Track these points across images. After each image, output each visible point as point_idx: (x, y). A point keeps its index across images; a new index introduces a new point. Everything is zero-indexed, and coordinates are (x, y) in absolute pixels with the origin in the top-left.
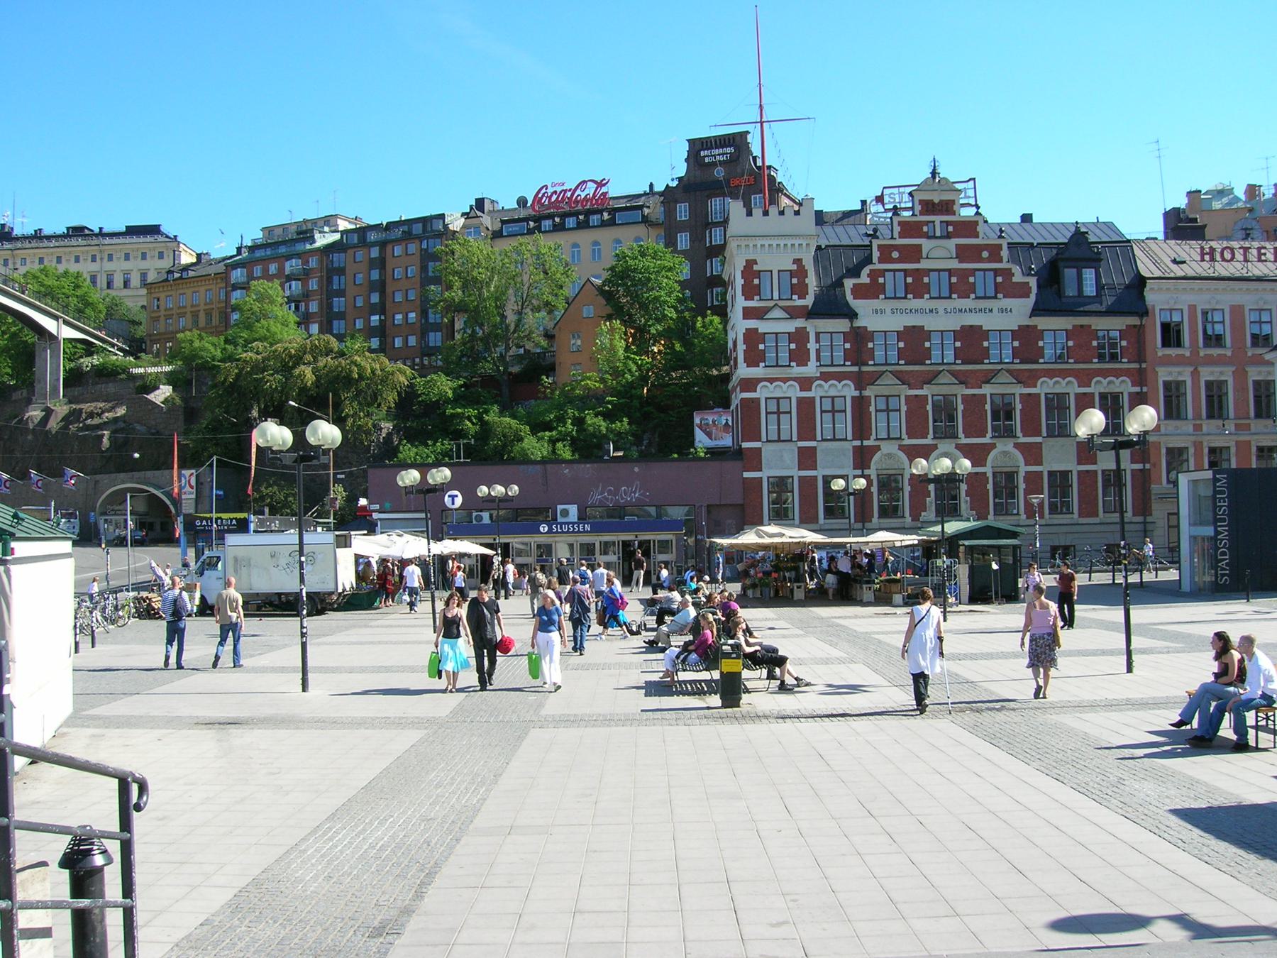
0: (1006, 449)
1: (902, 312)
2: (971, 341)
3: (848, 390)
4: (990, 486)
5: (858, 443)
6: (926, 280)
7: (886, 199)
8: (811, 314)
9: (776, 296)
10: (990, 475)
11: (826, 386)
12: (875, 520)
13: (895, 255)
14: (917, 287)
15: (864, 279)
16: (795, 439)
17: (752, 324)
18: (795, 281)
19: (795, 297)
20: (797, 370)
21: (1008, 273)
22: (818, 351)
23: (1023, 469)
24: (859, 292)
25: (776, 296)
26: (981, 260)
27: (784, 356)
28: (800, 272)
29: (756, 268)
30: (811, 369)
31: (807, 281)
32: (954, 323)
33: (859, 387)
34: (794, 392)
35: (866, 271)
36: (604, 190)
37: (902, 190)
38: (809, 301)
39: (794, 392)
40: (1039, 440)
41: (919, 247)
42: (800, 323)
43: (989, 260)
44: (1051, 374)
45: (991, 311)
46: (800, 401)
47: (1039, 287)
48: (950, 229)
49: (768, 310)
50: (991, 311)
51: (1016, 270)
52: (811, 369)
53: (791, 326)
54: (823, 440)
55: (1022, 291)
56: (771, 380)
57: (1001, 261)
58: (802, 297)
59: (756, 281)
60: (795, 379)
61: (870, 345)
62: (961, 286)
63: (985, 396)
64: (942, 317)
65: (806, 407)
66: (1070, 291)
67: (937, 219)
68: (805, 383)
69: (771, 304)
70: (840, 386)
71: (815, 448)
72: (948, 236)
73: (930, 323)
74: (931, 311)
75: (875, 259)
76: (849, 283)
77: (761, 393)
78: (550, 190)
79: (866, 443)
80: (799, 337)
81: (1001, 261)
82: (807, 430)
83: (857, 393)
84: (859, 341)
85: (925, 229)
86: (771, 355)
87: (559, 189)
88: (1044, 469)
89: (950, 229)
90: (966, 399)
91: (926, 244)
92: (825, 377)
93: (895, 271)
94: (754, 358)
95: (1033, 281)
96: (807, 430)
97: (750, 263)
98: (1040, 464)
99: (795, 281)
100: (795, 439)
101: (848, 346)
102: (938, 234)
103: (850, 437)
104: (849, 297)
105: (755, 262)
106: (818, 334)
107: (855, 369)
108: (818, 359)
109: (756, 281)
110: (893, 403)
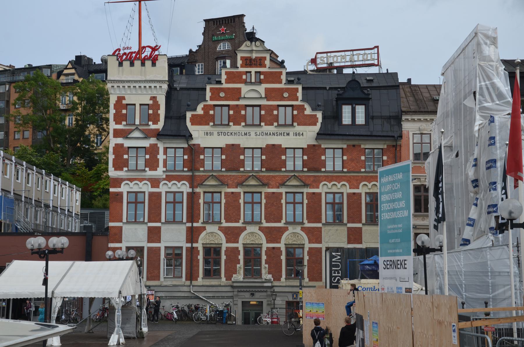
0: (294, 231)
1: (225, 134)
2: (273, 154)
3: (185, 188)
4: (283, 257)
5: (189, 225)
6: (243, 112)
7: (318, 61)
8: (160, 135)
9: (137, 122)
10: (283, 249)
11: (170, 184)
13: (222, 95)
14: (237, 118)
15: (200, 111)
16: (146, 221)
17: (120, 141)
18: (151, 112)
19: (150, 123)
20: (150, 173)
21: (301, 109)
22: (165, 161)
23: (308, 246)
24: (197, 121)
25: (137, 122)
26: (283, 99)
27: (141, 163)
28: (155, 106)
29: (124, 102)
30: (160, 172)
31: (159, 112)
32: (262, 142)
33: (192, 186)
34: (147, 188)
35: (200, 107)
36: (157, 53)
37: (329, 54)
38: (160, 126)
39: (147, 188)
40: (319, 225)
41: (239, 89)
42: (153, 141)
43: (288, 99)
44: (330, 179)
45: (288, 134)
46: (151, 194)
47: (324, 118)
48: (262, 77)
49: (131, 131)
50: (288, 134)
51: (307, 106)
52: (160, 172)
53: (146, 143)
54: (128, 222)
55: (312, 120)
56: (131, 180)
57: (297, 100)
58: (156, 122)
59: (124, 111)
60: (149, 180)
61: (202, 157)
62: (268, 117)
63: (281, 194)
64: (253, 139)
65: (155, 198)
66: (346, 120)
67: (253, 70)
68: (155, 182)
69: (133, 128)
70: (179, 184)
71: (159, 228)
72: (260, 82)
73: (243, 142)
74: (246, 134)
75: (208, 98)
76: (189, 115)
77: (124, 189)
78: (122, 52)
79: (195, 225)
80: (153, 151)
81: (297, 100)
82: (154, 216)
83: (190, 190)
84: (194, 153)
85: (244, 77)
86: (132, 163)
87: (127, 51)
88: (323, 246)
89: (262, 77)
90: (268, 196)
91: (245, 89)
92: (169, 178)
93: (285, 106)
94: (120, 164)
95: (319, 115)
96: (154, 216)
97: (120, 99)
98: (320, 242)
99: (151, 112)
100: (146, 221)
101: (186, 157)
102: (253, 81)
103: (185, 220)
105: (124, 98)
106: (166, 149)
107: (190, 174)
108: (165, 165)
109: (124, 111)
110: (298, 198)
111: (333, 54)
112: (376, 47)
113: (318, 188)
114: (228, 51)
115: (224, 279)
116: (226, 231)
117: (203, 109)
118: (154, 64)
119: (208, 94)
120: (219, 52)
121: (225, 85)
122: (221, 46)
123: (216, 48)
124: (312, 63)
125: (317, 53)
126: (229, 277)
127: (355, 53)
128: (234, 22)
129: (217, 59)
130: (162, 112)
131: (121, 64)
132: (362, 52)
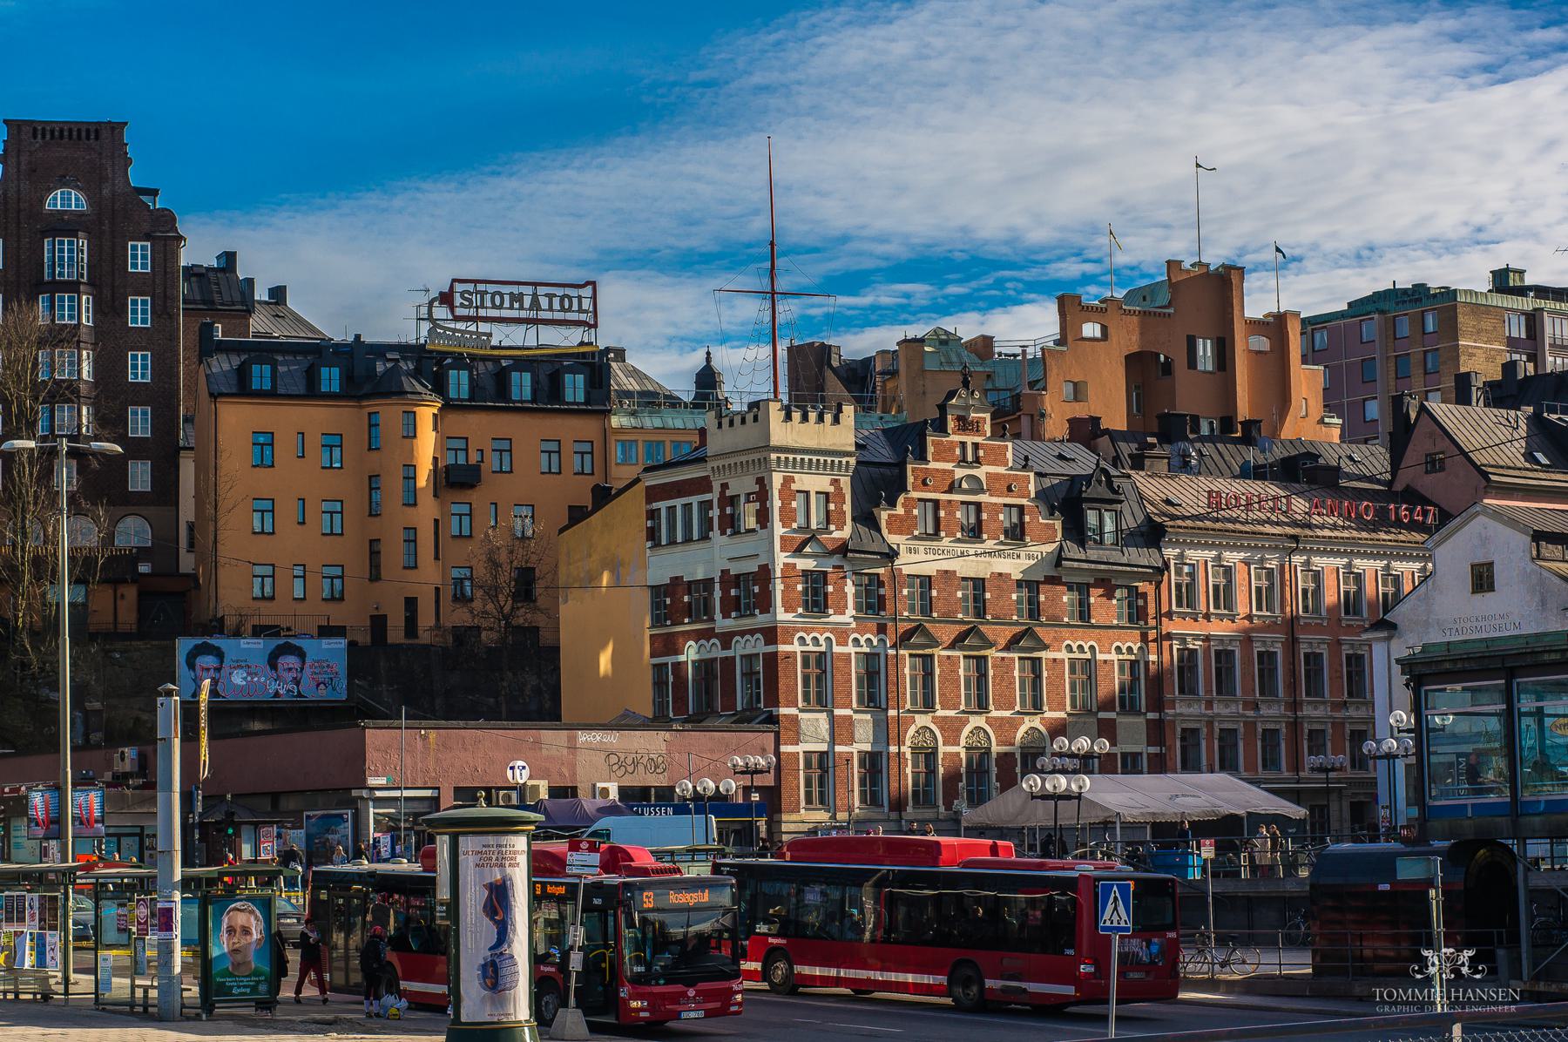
7: (458, 300)
12: (909, 809)
25: (814, 526)
29: (794, 487)
35: (901, 499)
37: (481, 287)
67: (969, 439)
75: (909, 487)
76: (884, 516)
95: (1058, 525)
102: (970, 458)
104: (885, 531)
111: (491, 288)
112: (588, 283)
114: (81, 215)
115: (942, 809)
117: (904, 505)
118: (836, 420)
119: (910, 479)
120: (52, 214)
121: (933, 465)
122: (55, 199)
123: (42, 201)
124: (441, 303)
125: (454, 280)
126: (948, 806)
127: (541, 290)
128: (97, 138)
129: (45, 233)
130: (847, 507)
131: (788, 417)
132: (560, 292)
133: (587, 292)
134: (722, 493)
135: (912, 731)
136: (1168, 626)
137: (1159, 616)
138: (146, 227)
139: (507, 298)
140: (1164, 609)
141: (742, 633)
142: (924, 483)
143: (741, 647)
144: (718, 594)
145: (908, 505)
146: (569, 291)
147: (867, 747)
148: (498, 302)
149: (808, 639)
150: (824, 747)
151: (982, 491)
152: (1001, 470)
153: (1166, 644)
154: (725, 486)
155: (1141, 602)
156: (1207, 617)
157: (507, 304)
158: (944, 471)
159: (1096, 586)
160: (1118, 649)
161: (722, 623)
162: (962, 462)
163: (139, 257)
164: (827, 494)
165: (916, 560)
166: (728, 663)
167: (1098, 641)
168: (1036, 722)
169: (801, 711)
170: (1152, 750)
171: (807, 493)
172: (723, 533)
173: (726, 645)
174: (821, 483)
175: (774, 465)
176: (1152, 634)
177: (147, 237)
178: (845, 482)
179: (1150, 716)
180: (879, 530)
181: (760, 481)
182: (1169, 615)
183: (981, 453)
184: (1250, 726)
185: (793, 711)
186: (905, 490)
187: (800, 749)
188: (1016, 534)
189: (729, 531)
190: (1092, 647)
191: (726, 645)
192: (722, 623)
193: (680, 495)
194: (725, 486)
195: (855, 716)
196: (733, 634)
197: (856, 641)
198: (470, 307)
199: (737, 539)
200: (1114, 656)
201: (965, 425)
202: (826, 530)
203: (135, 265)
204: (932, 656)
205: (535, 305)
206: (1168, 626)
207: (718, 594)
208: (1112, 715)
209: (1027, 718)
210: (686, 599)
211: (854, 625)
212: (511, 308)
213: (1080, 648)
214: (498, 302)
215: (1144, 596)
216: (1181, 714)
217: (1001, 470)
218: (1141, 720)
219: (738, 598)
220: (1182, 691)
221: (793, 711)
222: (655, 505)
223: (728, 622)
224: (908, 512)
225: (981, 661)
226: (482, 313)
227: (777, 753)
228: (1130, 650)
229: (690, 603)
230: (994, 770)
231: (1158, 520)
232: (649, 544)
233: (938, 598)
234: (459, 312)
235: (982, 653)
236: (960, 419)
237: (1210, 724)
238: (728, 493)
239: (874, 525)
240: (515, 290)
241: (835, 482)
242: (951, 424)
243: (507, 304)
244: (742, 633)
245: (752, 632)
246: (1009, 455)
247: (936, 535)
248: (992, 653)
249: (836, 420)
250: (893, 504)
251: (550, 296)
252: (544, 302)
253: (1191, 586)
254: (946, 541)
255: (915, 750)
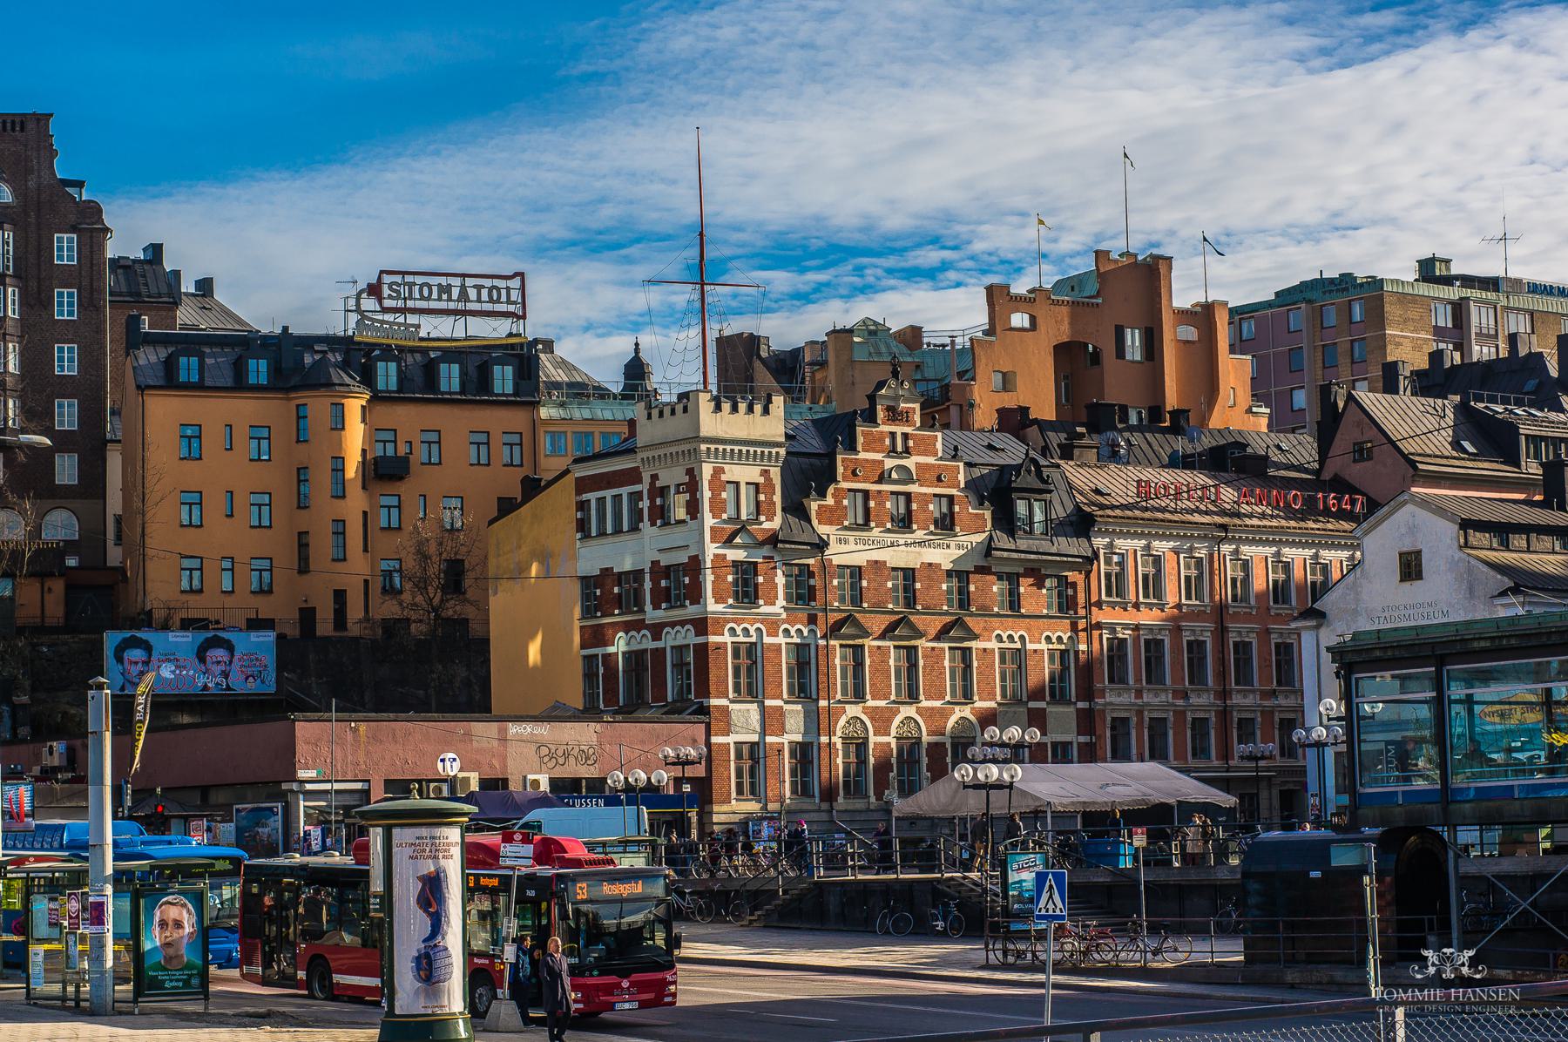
7: (386, 292)
12: (840, 799)
25: (744, 517)
29: (724, 478)
35: (831, 490)
37: (409, 279)
67: (899, 430)
75: (839, 478)
76: (814, 506)
95: (988, 514)
102: (899, 449)
104: (815, 522)
111: (419, 280)
113: (989, 640)
115: (873, 799)
116: (874, 713)
118: (766, 411)
119: (840, 470)
121: (862, 455)
125: (382, 272)
127: (469, 282)
128: (22, 130)
130: (777, 498)
131: (718, 408)
132: (488, 283)
133: (516, 283)
134: (652, 484)
135: (842, 721)
136: (1098, 616)
137: (1089, 605)
138: (72, 218)
139: (435, 289)
140: (1094, 599)
141: (673, 625)
142: (854, 473)
143: (671, 639)
144: (648, 585)
145: (838, 495)
146: (497, 282)
147: (799, 738)
148: (426, 293)
149: (739, 630)
150: (755, 738)
151: (911, 481)
152: (931, 460)
153: (1096, 633)
154: (654, 477)
155: (1070, 592)
156: (1137, 606)
157: (435, 295)
158: (874, 461)
159: (1025, 575)
160: (1048, 639)
161: (652, 615)
162: (892, 452)
163: (65, 248)
164: (757, 485)
165: (846, 550)
166: (659, 654)
167: (1028, 630)
168: (966, 712)
169: (732, 702)
170: (1082, 739)
171: (737, 484)
172: (653, 524)
173: (657, 637)
174: (746, 473)
175: (704, 456)
176: (1082, 624)
177: (73, 229)
178: (775, 474)
179: (1080, 705)
180: (809, 521)
181: (690, 472)
182: (1099, 604)
183: (911, 443)
184: (1180, 714)
185: (723, 702)
186: (835, 480)
187: (731, 739)
188: (946, 524)
189: (659, 522)
190: (1022, 638)
191: (657, 636)
192: (652, 615)
193: (610, 486)
194: (654, 477)
195: (787, 707)
196: (662, 625)
197: (786, 631)
198: (397, 298)
199: (667, 530)
200: (1043, 646)
201: (895, 415)
202: (757, 521)
203: (61, 258)
204: (862, 646)
205: (464, 296)
206: (1098, 616)
207: (648, 585)
208: (1042, 705)
209: (957, 708)
210: (616, 590)
211: (784, 616)
212: (440, 299)
213: (1010, 637)
214: (426, 293)
215: (1074, 585)
216: (1111, 704)
217: (931, 460)
218: (1072, 709)
219: (668, 589)
220: (1111, 680)
221: (723, 702)
222: (585, 497)
223: (660, 613)
224: (838, 502)
225: (911, 652)
226: (410, 304)
227: (708, 744)
228: (1060, 639)
229: (620, 595)
230: (925, 760)
231: (1086, 508)
232: (579, 535)
233: (868, 588)
234: (388, 303)
235: (913, 643)
236: (890, 409)
237: (1140, 713)
238: (658, 484)
239: (803, 515)
240: (443, 281)
241: (765, 473)
242: (881, 415)
243: (435, 295)
244: (673, 625)
245: (682, 623)
246: (939, 446)
247: (866, 526)
248: (922, 644)
249: (766, 411)
250: (823, 495)
251: (479, 288)
252: (472, 294)
253: (1121, 576)
254: (876, 532)
255: (846, 739)
